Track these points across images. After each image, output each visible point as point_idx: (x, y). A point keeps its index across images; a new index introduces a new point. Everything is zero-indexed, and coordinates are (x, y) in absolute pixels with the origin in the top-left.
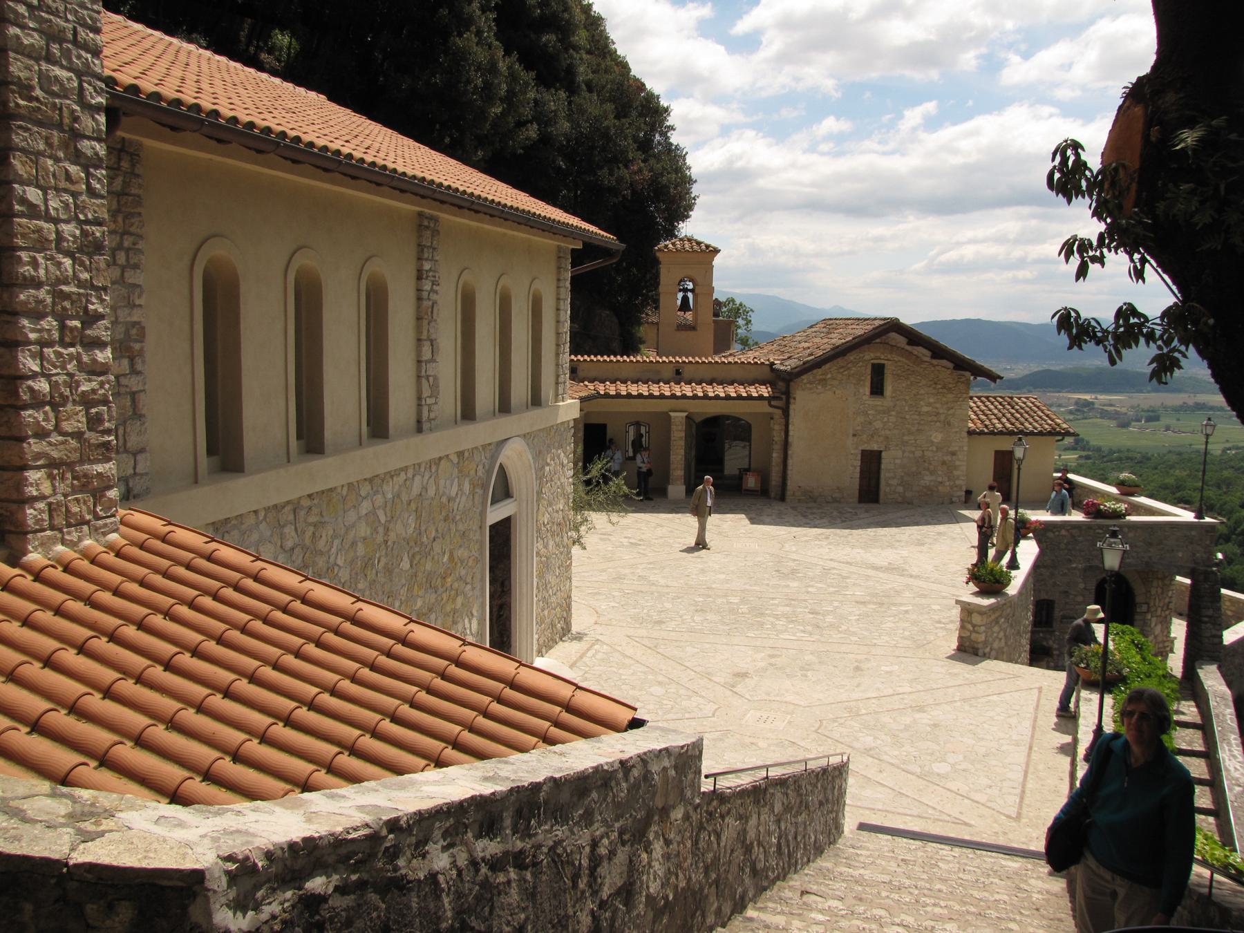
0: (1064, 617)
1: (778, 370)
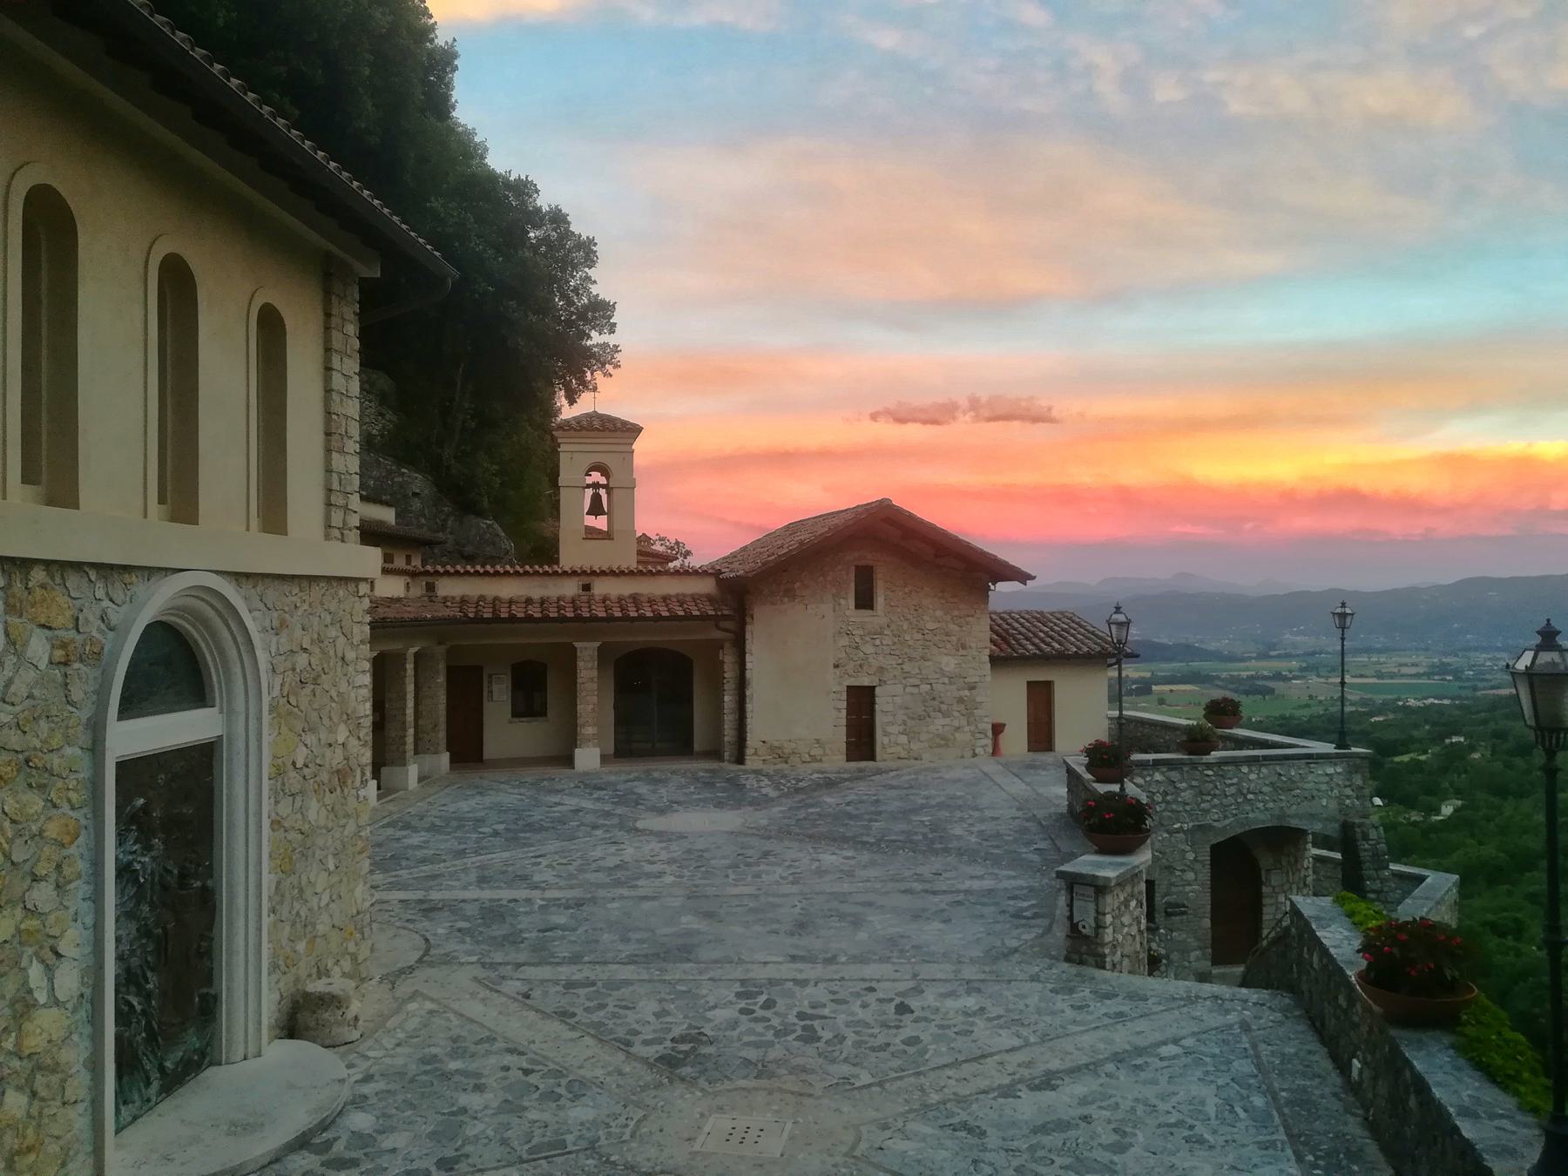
0: (1169, 904)
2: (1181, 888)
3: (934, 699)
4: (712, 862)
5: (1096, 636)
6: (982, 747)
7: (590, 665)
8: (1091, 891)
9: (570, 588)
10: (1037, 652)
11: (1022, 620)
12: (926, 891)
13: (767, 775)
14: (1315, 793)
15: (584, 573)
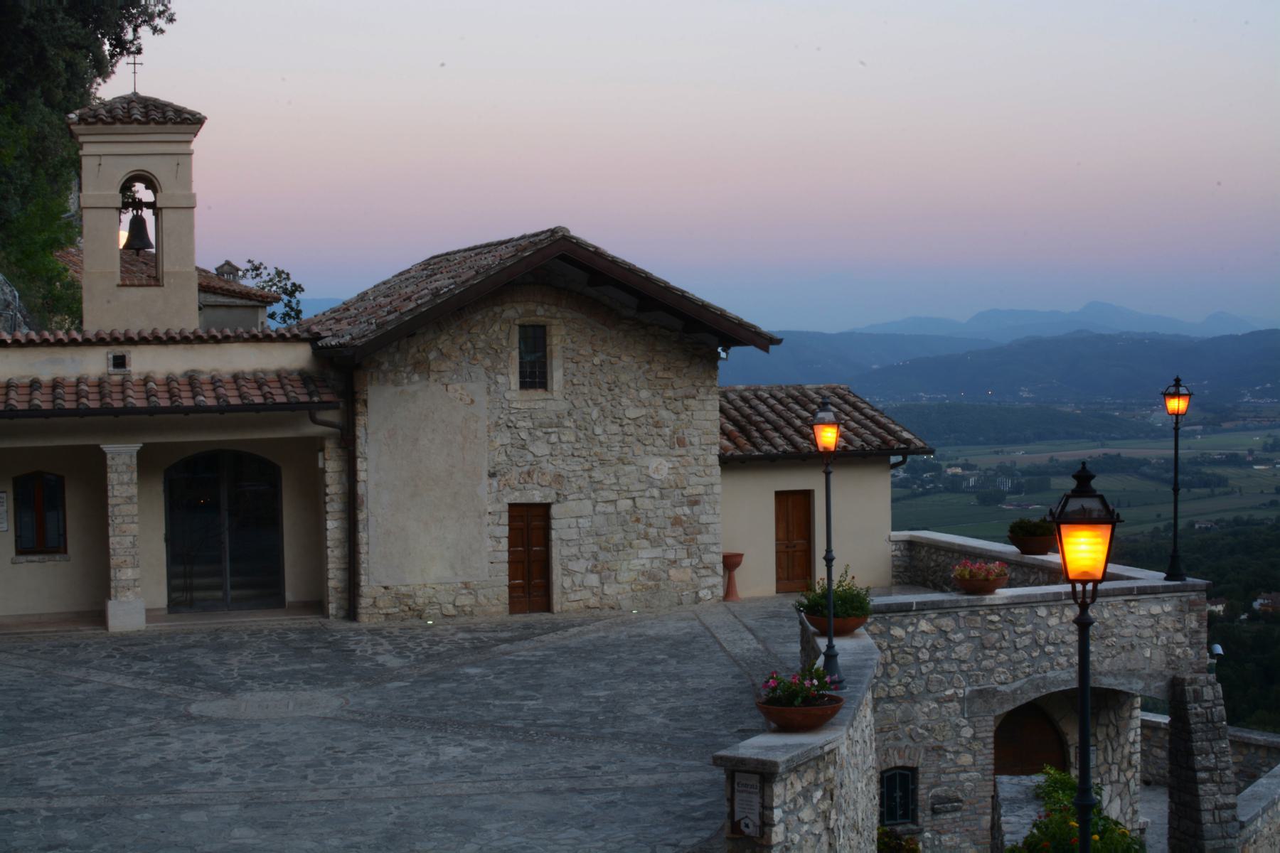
0: (939, 799)
1: (327, 348)
2: (954, 776)
3: (638, 520)
4: (287, 759)
5: (878, 424)
6: (709, 588)
7: (126, 478)
8: (755, 780)
9: (94, 364)
10: (789, 448)
11: (772, 401)
12: (572, 790)
13: (390, 638)
14: (1136, 641)
15: (115, 341)
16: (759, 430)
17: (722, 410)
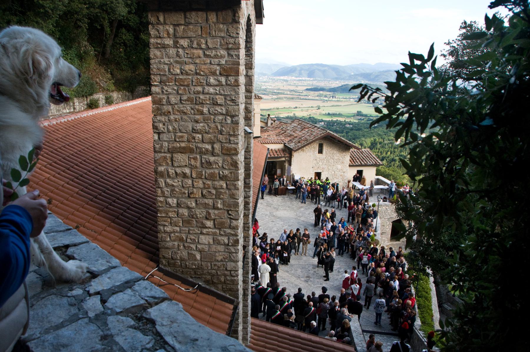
16: (355, 159)
17: (350, 156)
